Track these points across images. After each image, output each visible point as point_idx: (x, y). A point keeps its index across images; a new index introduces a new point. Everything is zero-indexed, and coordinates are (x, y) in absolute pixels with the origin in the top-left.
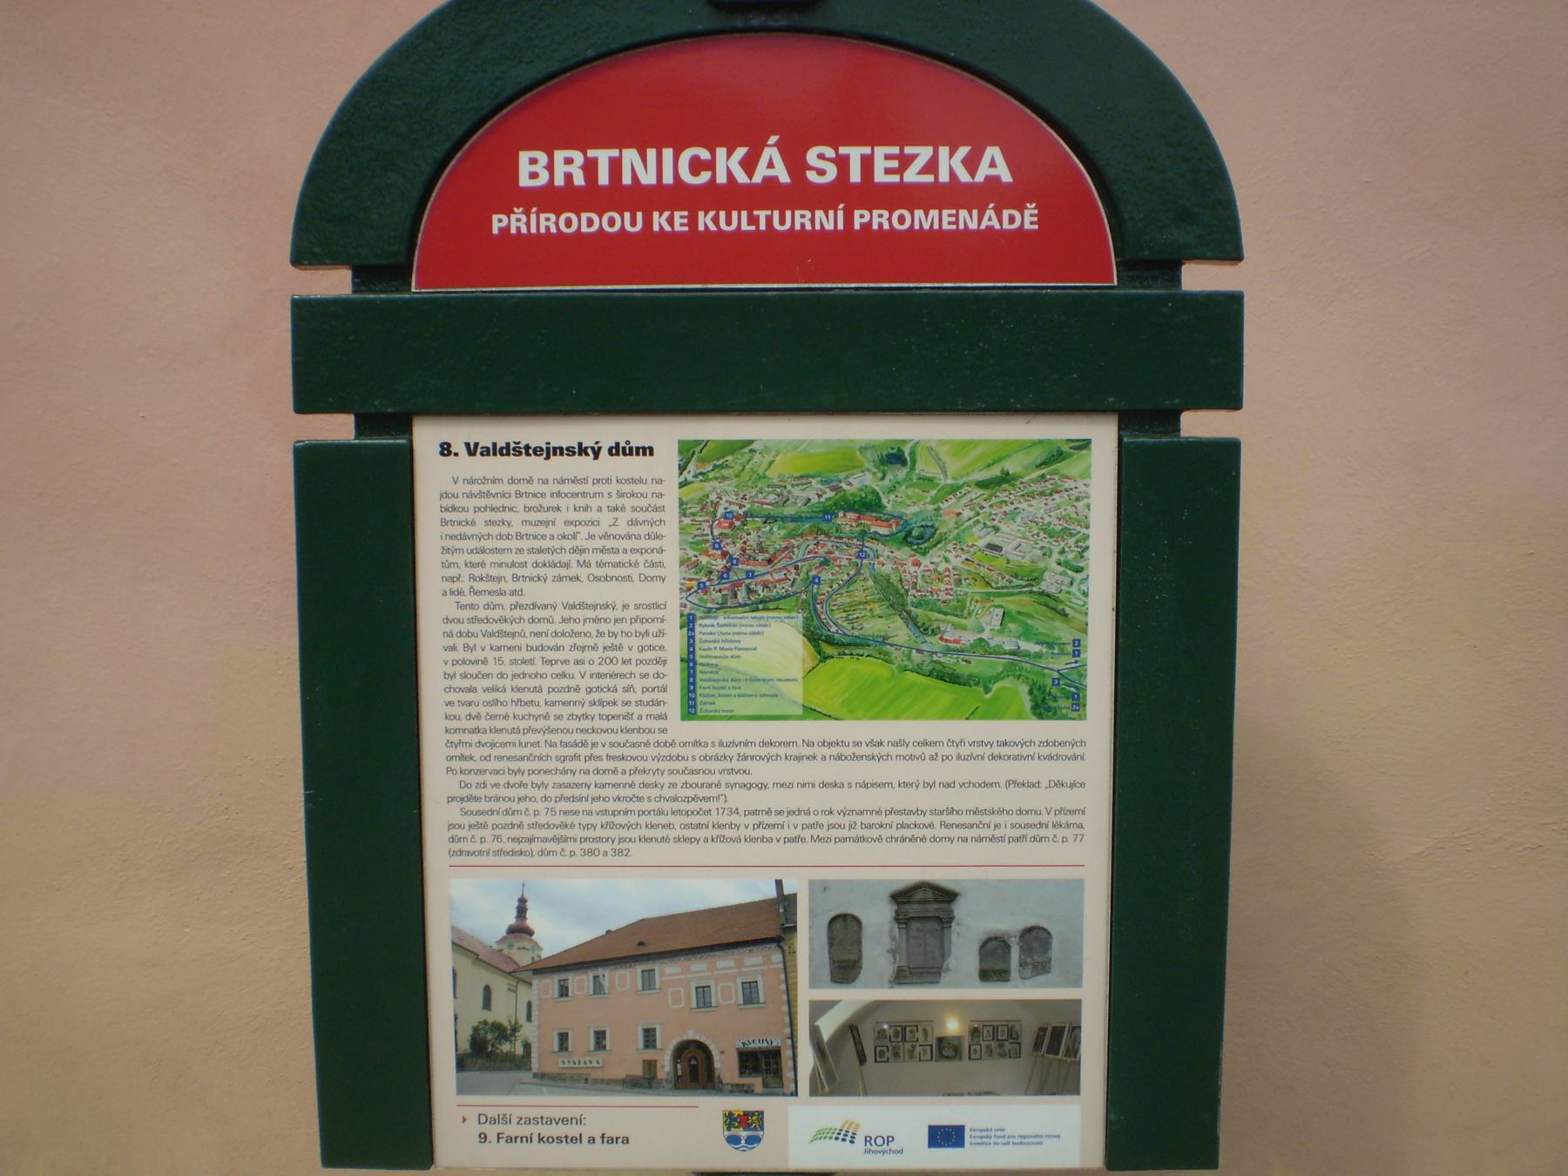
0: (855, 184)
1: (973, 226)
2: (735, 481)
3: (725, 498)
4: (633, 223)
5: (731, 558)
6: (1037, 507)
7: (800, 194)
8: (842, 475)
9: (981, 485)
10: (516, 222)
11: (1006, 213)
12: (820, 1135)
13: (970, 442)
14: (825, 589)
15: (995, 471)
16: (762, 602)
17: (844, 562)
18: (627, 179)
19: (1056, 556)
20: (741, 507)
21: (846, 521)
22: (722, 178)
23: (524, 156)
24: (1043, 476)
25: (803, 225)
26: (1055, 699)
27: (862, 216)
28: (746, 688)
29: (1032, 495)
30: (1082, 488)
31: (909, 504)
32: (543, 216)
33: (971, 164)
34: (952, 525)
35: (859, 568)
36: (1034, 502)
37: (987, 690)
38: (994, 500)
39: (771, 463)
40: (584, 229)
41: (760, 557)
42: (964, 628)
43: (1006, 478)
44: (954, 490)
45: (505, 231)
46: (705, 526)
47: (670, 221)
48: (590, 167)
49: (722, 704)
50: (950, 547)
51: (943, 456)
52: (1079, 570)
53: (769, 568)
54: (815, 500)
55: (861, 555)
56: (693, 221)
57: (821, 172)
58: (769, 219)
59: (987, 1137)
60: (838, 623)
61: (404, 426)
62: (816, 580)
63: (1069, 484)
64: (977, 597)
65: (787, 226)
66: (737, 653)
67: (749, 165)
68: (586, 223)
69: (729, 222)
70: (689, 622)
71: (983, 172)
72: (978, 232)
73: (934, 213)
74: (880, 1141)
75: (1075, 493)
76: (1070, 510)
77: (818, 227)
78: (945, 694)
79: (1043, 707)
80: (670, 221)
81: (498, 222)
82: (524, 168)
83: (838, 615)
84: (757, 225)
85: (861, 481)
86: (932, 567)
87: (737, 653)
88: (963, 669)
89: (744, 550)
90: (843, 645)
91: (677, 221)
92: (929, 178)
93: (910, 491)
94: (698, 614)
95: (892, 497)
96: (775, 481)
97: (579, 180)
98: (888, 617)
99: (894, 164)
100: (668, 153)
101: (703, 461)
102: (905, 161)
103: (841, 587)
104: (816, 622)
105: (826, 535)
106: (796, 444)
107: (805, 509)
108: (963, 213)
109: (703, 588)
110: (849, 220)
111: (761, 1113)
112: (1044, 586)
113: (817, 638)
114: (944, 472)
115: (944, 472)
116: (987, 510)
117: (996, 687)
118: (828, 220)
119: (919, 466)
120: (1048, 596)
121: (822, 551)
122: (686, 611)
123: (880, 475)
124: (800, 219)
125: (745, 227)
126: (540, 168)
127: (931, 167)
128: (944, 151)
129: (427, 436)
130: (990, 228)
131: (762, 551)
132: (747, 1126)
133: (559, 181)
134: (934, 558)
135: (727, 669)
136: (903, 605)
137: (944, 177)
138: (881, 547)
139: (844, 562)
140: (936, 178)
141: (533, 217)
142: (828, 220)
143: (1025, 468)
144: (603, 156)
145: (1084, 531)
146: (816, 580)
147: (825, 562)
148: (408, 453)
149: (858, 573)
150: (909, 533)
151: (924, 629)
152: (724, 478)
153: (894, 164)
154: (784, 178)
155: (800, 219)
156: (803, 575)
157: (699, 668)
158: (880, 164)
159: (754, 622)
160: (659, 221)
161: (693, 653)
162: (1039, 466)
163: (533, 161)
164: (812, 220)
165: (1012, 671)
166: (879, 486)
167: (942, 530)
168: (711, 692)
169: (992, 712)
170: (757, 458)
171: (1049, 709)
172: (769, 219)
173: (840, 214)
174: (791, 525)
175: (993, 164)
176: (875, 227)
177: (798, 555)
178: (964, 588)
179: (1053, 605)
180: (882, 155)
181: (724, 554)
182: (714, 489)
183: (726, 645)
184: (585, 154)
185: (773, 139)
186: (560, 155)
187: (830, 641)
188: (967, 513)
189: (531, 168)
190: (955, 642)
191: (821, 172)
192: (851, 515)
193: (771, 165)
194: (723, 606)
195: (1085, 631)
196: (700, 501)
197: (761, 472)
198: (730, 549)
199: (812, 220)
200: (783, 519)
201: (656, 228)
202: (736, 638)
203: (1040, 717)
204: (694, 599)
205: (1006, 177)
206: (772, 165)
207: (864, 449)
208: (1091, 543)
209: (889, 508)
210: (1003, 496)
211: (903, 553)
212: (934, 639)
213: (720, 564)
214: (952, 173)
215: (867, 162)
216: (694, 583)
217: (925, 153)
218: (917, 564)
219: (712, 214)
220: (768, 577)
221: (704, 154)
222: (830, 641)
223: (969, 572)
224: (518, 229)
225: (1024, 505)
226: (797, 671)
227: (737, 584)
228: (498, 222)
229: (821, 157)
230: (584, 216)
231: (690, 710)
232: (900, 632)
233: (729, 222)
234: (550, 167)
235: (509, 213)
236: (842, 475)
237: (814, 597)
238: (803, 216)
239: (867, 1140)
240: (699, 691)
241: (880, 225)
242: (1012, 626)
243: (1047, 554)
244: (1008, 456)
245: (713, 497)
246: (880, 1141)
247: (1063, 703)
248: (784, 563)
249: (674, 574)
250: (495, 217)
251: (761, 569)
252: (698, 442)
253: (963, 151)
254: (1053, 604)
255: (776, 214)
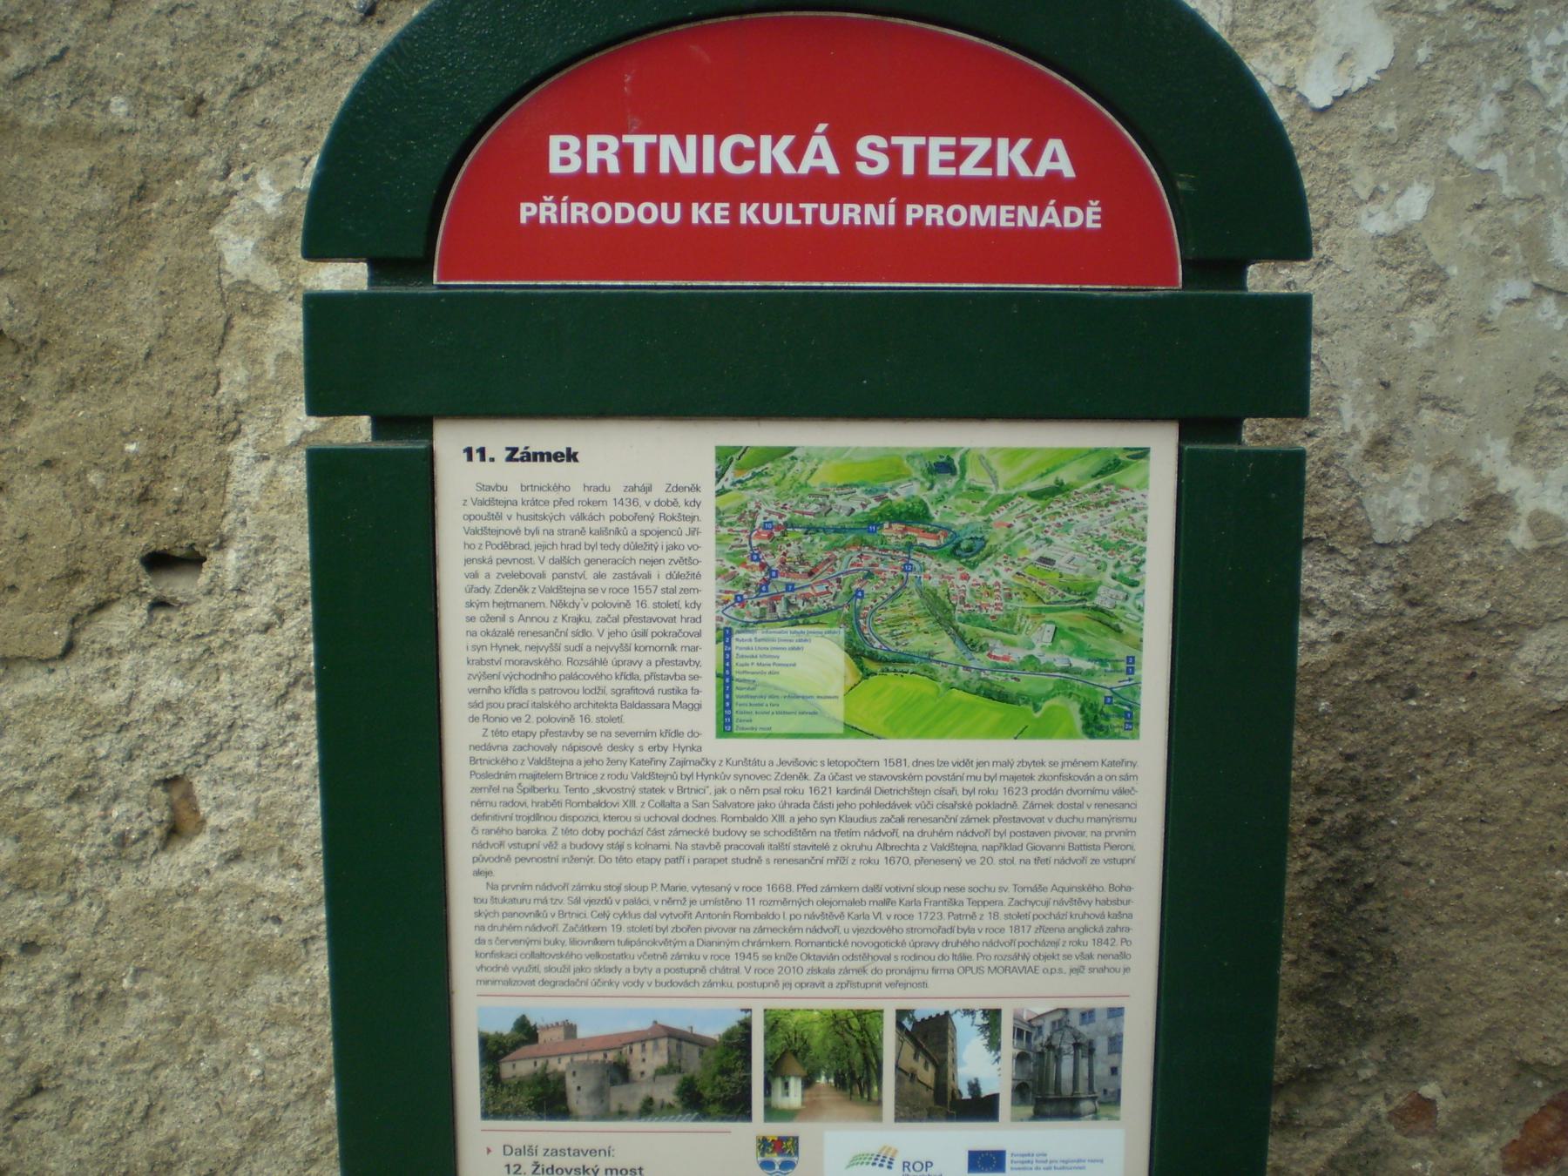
0: (908, 177)
1: (1032, 223)
2: (775, 490)
3: (764, 507)
4: (671, 215)
5: (770, 570)
6: (1091, 519)
7: (850, 187)
8: (888, 485)
9: (1034, 495)
10: (546, 211)
11: (1067, 210)
12: (857, 1160)
13: (1023, 450)
14: (868, 602)
15: (1049, 481)
16: (802, 616)
17: (889, 575)
18: (664, 168)
19: (1110, 570)
20: (781, 516)
21: (892, 533)
22: (766, 169)
23: (555, 141)
24: (1098, 487)
25: (851, 220)
26: (1107, 717)
27: (915, 211)
28: (785, 706)
29: (1086, 506)
30: (1139, 499)
31: (957, 514)
32: (574, 205)
33: (1032, 157)
34: (1002, 537)
35: (904, 581)
36: (1089, 514)
37: (1036, 708)
38: (1048, 511)
39: (813, 471)
40: (619, 220)
41: (801, 569)
42: (1013, 644)
43: (1059, 489)
44: (1005, 500)
45: (534, 220)
46: (743, 536)
47: (711, 213)
48: (626, 154)
49: (759, 721)
50: (1000, 560)
51: (993, 465)
52: (1134, 584)
53: (809, 581)
54: (859, 510)
55: (907, 567)
56: (734, 214)
57: (872, 164)
58: (816, 213)
59: (1027, 1160)
60: (880, 638)
61: (422, 426)
62: (859, 594)
63: (1126, 494)
64: (1028, 612)
65: (835, 220)
66: (776, 668)
67: (795, 154)
68: (621, 213)
69: (773, 215)
70: (725, 636)
71: (1044, 166)
72: (1037, 230)
73: (991, 209)
74: (918, 1166)
75: (1132, 504)
76: (1127, 521)
77: (867, 222)
78: (993, 712)
79: (1094, 726)
80: (711, 213)
81: (526, 211)
82: (555, 154)
83: (883, 631)
84: (803, 220)
85: (907, 491)
86: (981, 581)
87: (776, 668)
88: (1012, 687)
89: (783, 562)
90: (887, 661)
91: (718, 213)
92: (987, 172)
93: (959, 502)
94: (735, 629)
95: (940, 508)
96: (817, 491)
97: (614, 167)
98: (935, 632)
99: (950, 156)
100: (709, 140)
101: (741, 469)
102: (962, 153)
103: (885, 601)
104: (858, 637)
105: (871, 547)
106: (840, 452)
107: (849, 519)
108: (1022, 210)
109: (740, 601)
110: (900, 214)
111: (796, 1139)
112: (1097, 601)
113: (858, 653)
114: (995, 480)
115: (995, 482)
116: (1040, 521)
117: (1045, 706)
118: (878, 215)
119: (969, 475)
120: (1102, 611)
121: (865, 563)
122: (723, 625)
123: (928, 485)
124: (849, 213)
125: (790, 221)
126: (571, 154)
127: (989, 160)
128: (1003, 143)
129: (449, 440)
130: (1050, 227)
131: (803, 562)
132: (781, 1152)
133: (592, 168)
134: (984, 572)
135: (765, 685)
136: (951, 621)
137: (1003, 171)
138: (927, 560)
139: (889, 575)
140: (995, 171)
141: (564, 206)
142: (878, 215)
143: (1080, 477)
144: (640, 142)
145: (1141, 544)
146: (859, 594)
147: (869, 575)
148: (429, 456)
149: (903, 587)
150: (958, 546)
151: (972, 646)
152: (763, 486)
153: (950, 156)
154: (833, 169)
155: (849, 213)
156: (845, 589)
157: (735, 684)
158: (935, 156)
159: (795, 637)
160: (699, 213)
161: (730, 668)
162: (1094, 476)
163: (565, 146)
164: (862, 215)
165: (1064, 689)
166: (926, 496)
167: (992, 543)
168: (748, 709)
169: (1042, 731)
170: (799, 465)
171: (1101, 728)
172: (816, 213)
173: (892, 208)
174: (834, 536)
175: (1054, 158)
176: (929, 222)
177: (840, 567)
178: (1014, 603)
179: (1106, 620)
180: (938, 148)
181: (763, 566)
182: (753, 498)
183: (765, 661)
184: (620, 139)
185: (821, 127)
186: (593, 140)
187: (873, 657)
188: (1019, 525)
189: (563, 154)
190: (1005, 659)
191: (872, 164)
192: (897, 526)
193: (818, 155)
194: (761, 620)
195: (1138, 646)
196: (738, 510)
197: (802, 480)
198: (770, 561)
199: (862, 215)
200: (826, 530)
201: (695, 220)
202: (775, 653)
203: (1091, 736)
204: (731, 612)
205: (1069, 172)
206: (820, 155)
207: (911, 457)
208: (1147, 556)
209: (937, 519)
210: (1056, 507)
211: (951, 567)
212: (982, 656)
213: (758, 576)
214: (1011, 167)
215: (921, 154)
216: (731, 596)
217: (982, 145)
218: (965, 577)
219: (755, 206)
220: (809, 590)
221: (748, 142)
222: (873, 657)
223: (1020, 586)
224: (548, 218)
225: (1078, 517)
226: (837, 687)
227: (776, 597)
228: (526, 211)
229: (872, 147)
230: (619, 206)
231: (726, 727)
232: (946, 648)
233: (773, 215)
234: (583, 153)
235: (538, 201)
236: (888, 485)
237: (857, 612)
238: (852, 210)
239: (906, 1165)
240: (735, 708)
241: (934, 221)
242: (1063, 642)
243: (1101, 567)
244: (1063, 465)
245: (752, 506)
246: (918, 1166)
247: (1115, 722)
248: (825, 576)
249: (709, 589)
250: (524, 206)
251: (801, 582)
252: (737, 449)
253: (1023, 143)
254: (1107, 619)
255: (823, 207)
